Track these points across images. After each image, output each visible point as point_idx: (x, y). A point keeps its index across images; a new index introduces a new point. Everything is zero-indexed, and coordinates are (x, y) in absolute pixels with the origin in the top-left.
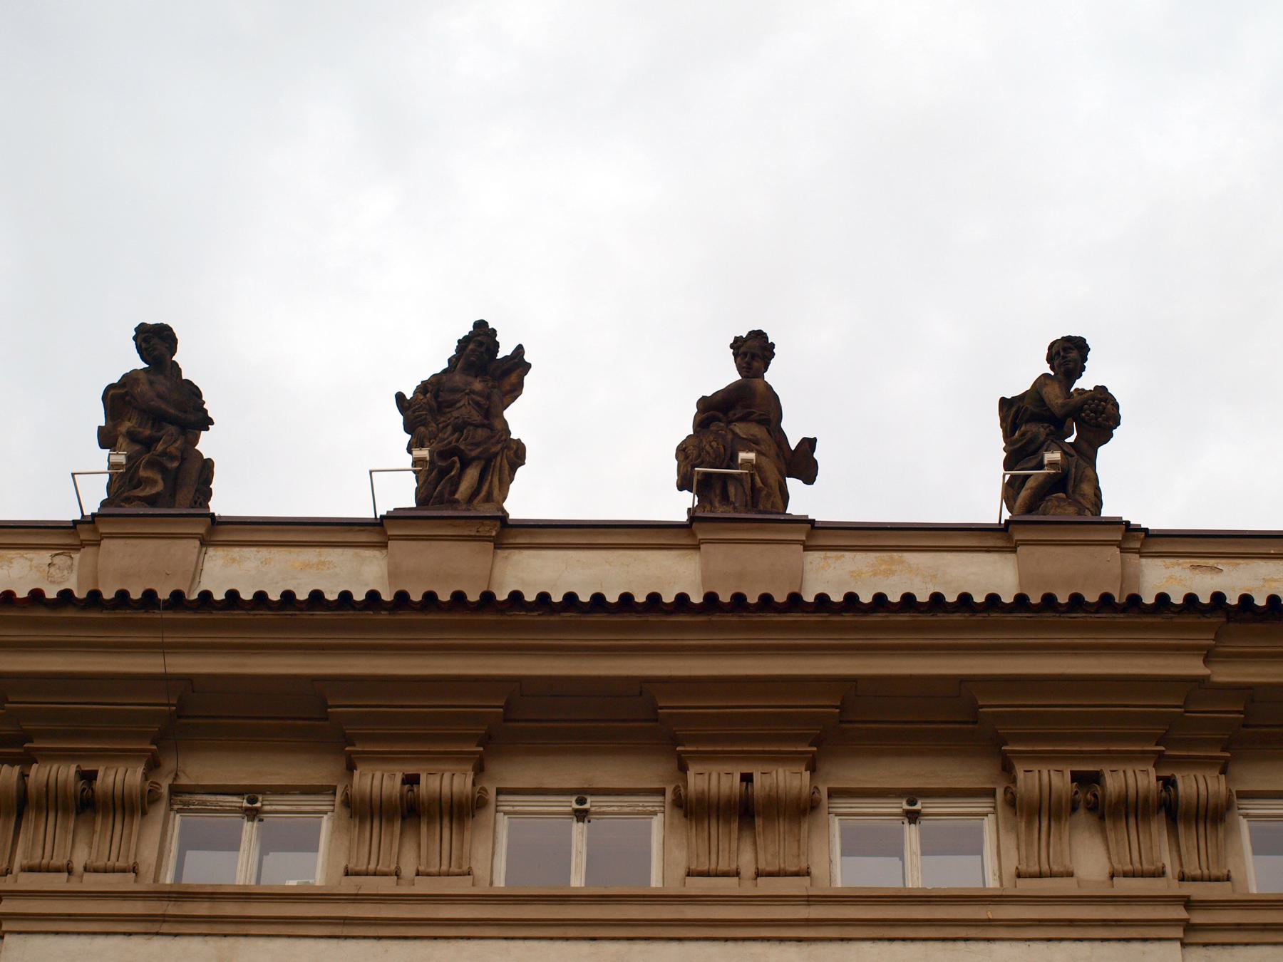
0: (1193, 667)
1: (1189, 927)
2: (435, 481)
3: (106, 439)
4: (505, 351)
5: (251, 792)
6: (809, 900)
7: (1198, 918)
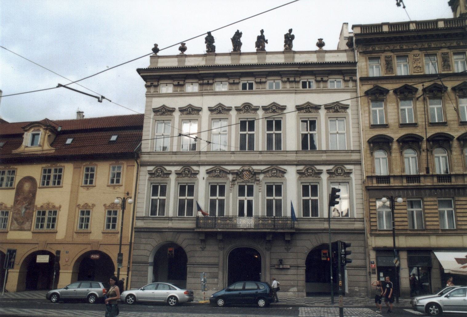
1: (296, 92)
2: (235, 50)
3: (206, 43)
4: (240, 32)
5: (221, 82)
6: (265, 91)
7: (296, 92)
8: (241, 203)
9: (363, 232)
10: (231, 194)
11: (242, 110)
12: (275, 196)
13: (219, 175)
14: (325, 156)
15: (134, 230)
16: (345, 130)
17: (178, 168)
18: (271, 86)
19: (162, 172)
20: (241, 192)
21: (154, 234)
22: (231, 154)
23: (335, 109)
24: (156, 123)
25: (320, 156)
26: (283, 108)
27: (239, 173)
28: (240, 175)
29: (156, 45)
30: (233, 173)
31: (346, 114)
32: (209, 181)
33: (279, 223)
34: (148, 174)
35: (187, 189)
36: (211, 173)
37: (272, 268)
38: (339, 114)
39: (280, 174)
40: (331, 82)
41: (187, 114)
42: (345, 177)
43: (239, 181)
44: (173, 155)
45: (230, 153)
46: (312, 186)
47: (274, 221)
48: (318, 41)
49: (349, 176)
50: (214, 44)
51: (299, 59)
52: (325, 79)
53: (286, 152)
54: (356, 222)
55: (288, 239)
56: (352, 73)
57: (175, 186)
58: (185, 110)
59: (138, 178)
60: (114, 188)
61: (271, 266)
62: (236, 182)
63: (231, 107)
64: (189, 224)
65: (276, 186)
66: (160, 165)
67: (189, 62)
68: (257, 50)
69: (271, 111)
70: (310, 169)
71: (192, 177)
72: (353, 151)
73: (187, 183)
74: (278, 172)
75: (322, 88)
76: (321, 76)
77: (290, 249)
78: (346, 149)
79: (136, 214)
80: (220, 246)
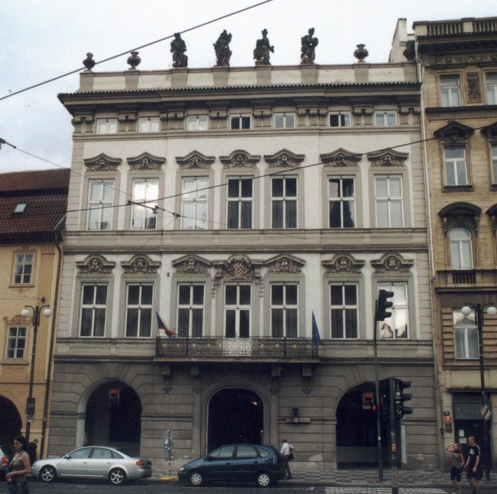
0: (322, 94)
1: (320, 133)
2: (219, 63)
3: (172, 51)
4: (228, 33)
5: (197, 115)
7: (321, 132)
8: (231, 316)
9: (432, 363)
10: (214, 301)
11: (232, 163)
12: (286, 304)
13: (193, 270)
14: (368, 237)
15: (53, 360)
16: (402, 195)
17: (127, 258)
18: (279, 123)
19: (99, 264)
20: (230, 297)
21: (87, 366)
22: (213, 234)
23: (385, 161)
24: (90, 183)
25: (360, 238)
26: (299, 159)
27: (227, 266)
28: (228, 270)
29: (90, 55)
30: (216, 267)
31: (403, 168)
32: (178, 279)
33: (293, 349)
34: (76, 267)
35: (140, 293)
36: (180, 266)
37: (280, 422)
38: (391, 168)
39: (295, 268)
40: (378, 116)
41: (141, 169)
42: (401, 272)
43: (227, 279)
44: (118, 237)
45: (212, 232)
46: (346, 287)
47: (285, 345)
48: (357, 48)
49: (408, 272)
50: (186, 53)
51: (325, 78)
52: (368, 110)
53: (304, 232)
54: (419, 347)
55: (308, 375)
56: (413, 101)
57: (121, 287)
58: (138, 162)
59: (61, 274)
60: (21, 291)
61: (279, 420)
62: (222, 281)
63: (214, 157)
64: (144, 351)
65: (287, 287)
66: (96, 253)
67: (145, 84)
68: (256, 63)
69: (279, 164)
70: (344, 259)
71: (149, 273)
72: (414, 230)
73: (141, 283)
74: (292, 264)
75: (363, 126)
76: (362, 107)
77: (311, 391)
78: (404, 227)
79: (57, 335)
80: (195, 386)
